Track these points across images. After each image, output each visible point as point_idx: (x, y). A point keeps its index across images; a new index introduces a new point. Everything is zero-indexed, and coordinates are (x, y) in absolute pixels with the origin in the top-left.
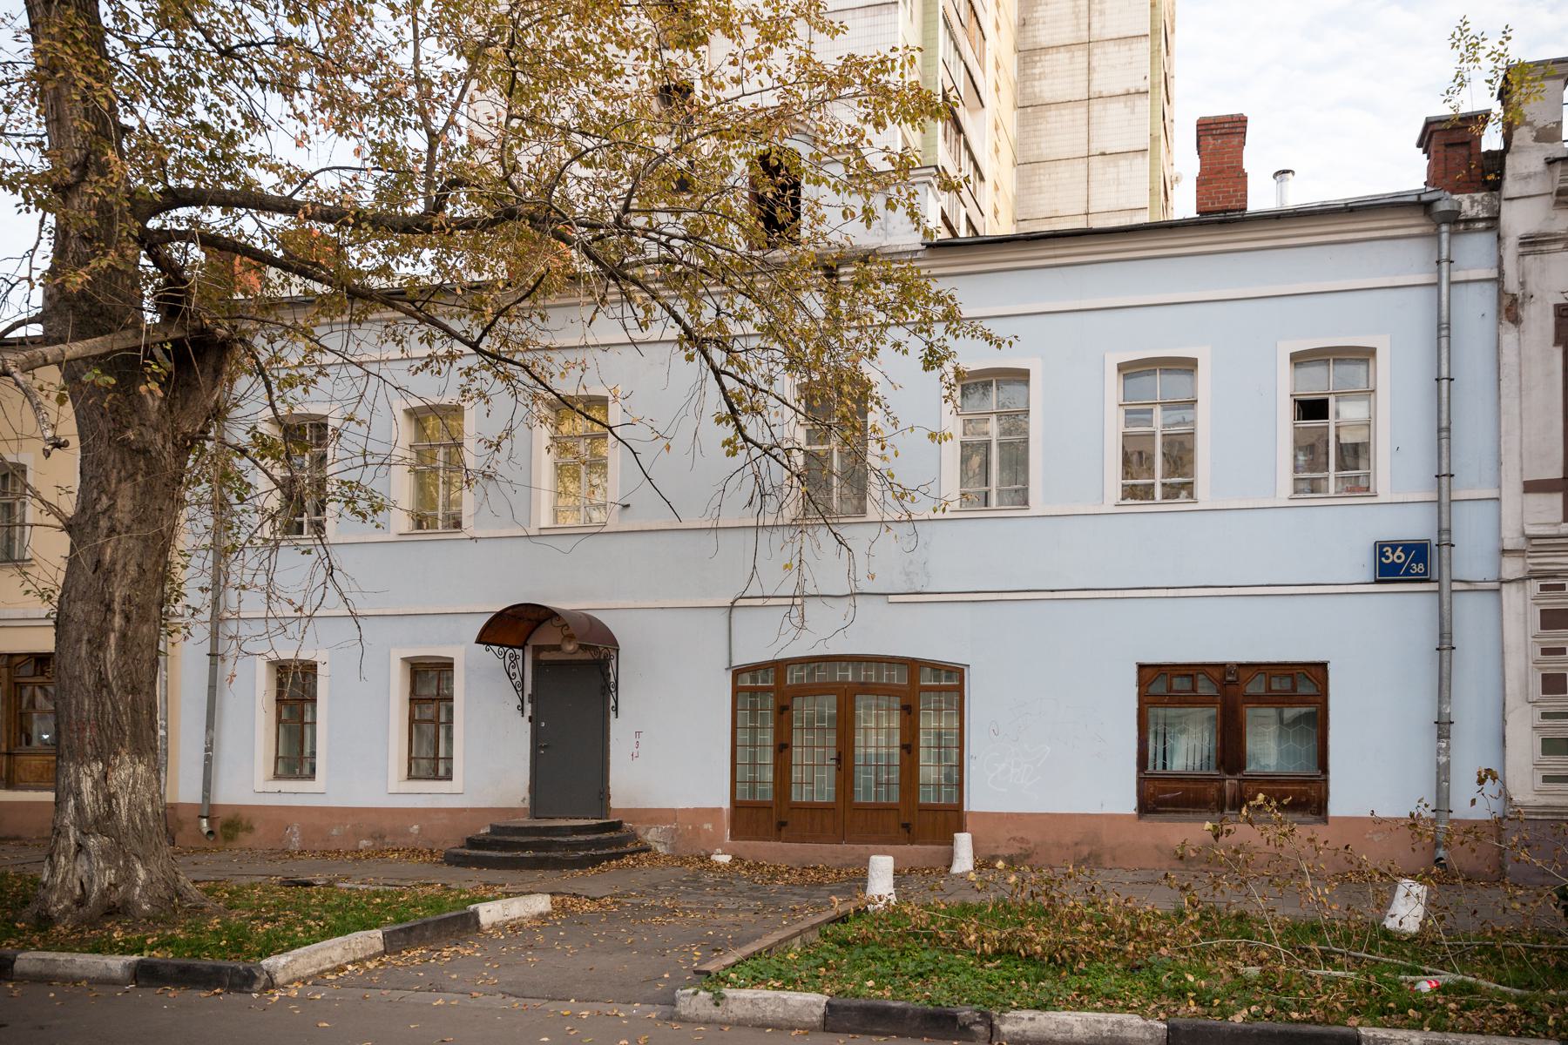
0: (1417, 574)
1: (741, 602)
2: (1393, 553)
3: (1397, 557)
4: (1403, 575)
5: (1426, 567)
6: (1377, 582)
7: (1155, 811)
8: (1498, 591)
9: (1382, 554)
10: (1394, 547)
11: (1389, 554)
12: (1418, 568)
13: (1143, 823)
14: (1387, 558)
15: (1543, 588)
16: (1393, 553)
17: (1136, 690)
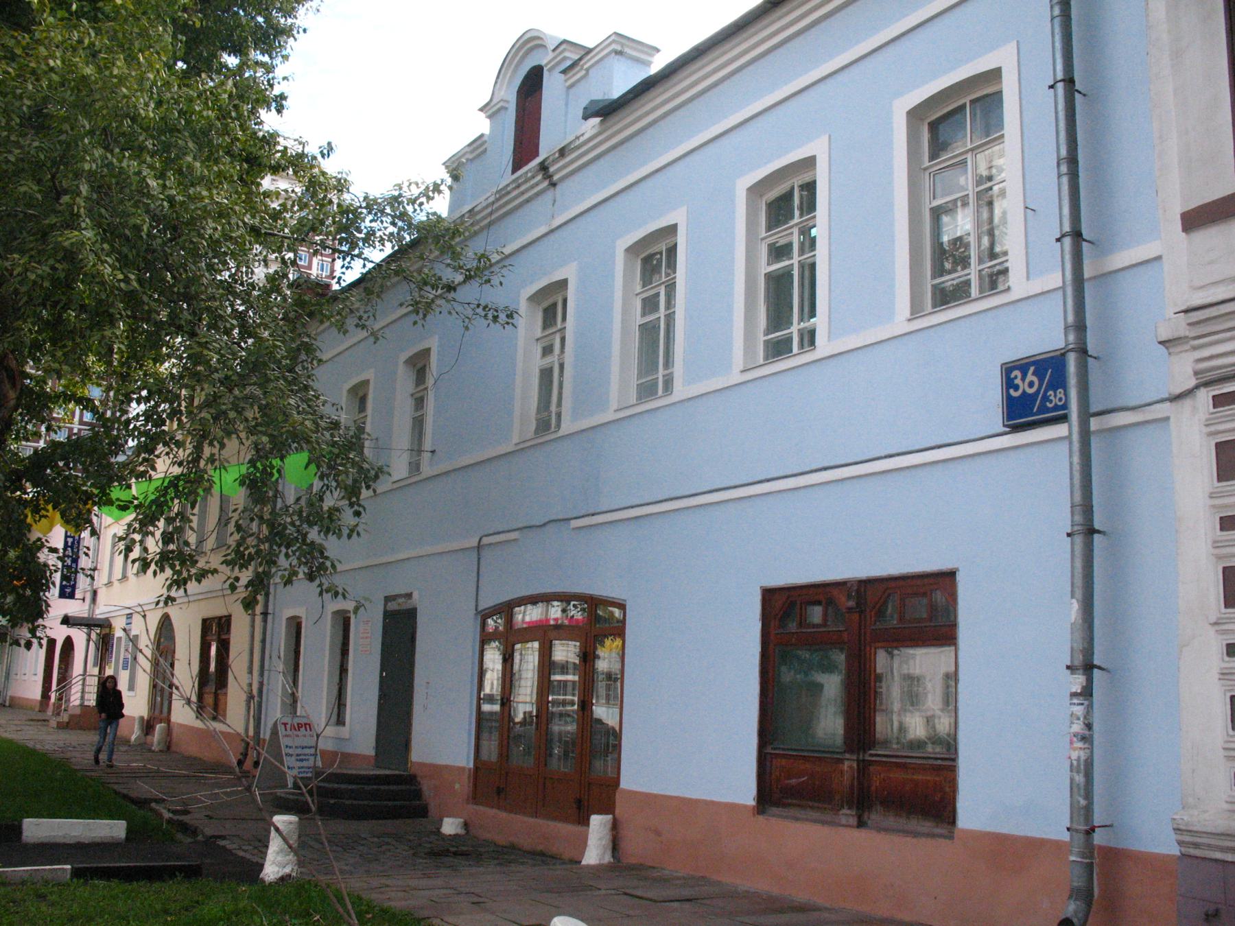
0: (1056, 408)
1: (485, 541)
2: (1023, 379)
3: (1027, 384)
4: (1040, 412)
5: (1065, 395)
6: (1016, 429)
7: (778, 804)
8: (1167, 419)
9: (1009, 384)
10: (1022, 366)
11: (1018, 381)
12: (1055, 398)
13: (761, 818)
14: (1016, 388)
15: (1219, 401)
16: (1023, 379)
17: (758, 626)
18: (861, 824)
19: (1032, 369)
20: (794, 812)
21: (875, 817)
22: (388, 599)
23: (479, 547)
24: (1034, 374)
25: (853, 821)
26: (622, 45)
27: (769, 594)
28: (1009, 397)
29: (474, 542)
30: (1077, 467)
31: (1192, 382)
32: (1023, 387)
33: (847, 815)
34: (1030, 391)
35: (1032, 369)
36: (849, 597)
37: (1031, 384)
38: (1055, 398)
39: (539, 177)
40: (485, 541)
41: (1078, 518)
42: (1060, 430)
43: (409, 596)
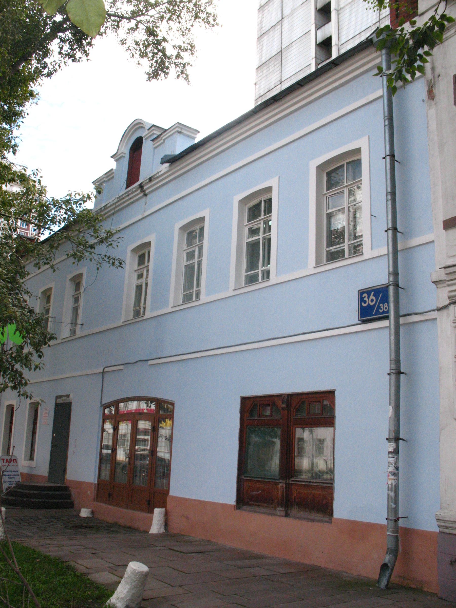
0: (384, 312)
1: (106, 369)
2: (368, 298)
3: (371, 300)
4: (375, 315)
5: (388, 306)
6: (365, 322)
7: (248, 504)
9: (361, 300)
10: (368, 291)
11: (366, 299)
12: (383, 307)
13: (238, 511)
14: (365, 302)
16: (368, 298)
17: (239, 415)
18: (287, 515)
19: (373, 293)
20: (256, 509)
21: (294, 511)
22: (57, 397)
23: (103, 372)
24: (373, 296)
25: (283, 513)
26: (182, 129)
27: (244, 400)
28: (361, 305)
29: (101, 370)
30: (393, 342)
31: (447, 302)
32: (368, 302)
33: (280, 510)
34: (372, 304)
35: (373, 293)
36: (283, 403)
37: (372, 301)
38: (383, 307)
39: (139, 191)
40: (106, 369)
41: (393, 366)
42: (385, 323)
43: (68, 396)
